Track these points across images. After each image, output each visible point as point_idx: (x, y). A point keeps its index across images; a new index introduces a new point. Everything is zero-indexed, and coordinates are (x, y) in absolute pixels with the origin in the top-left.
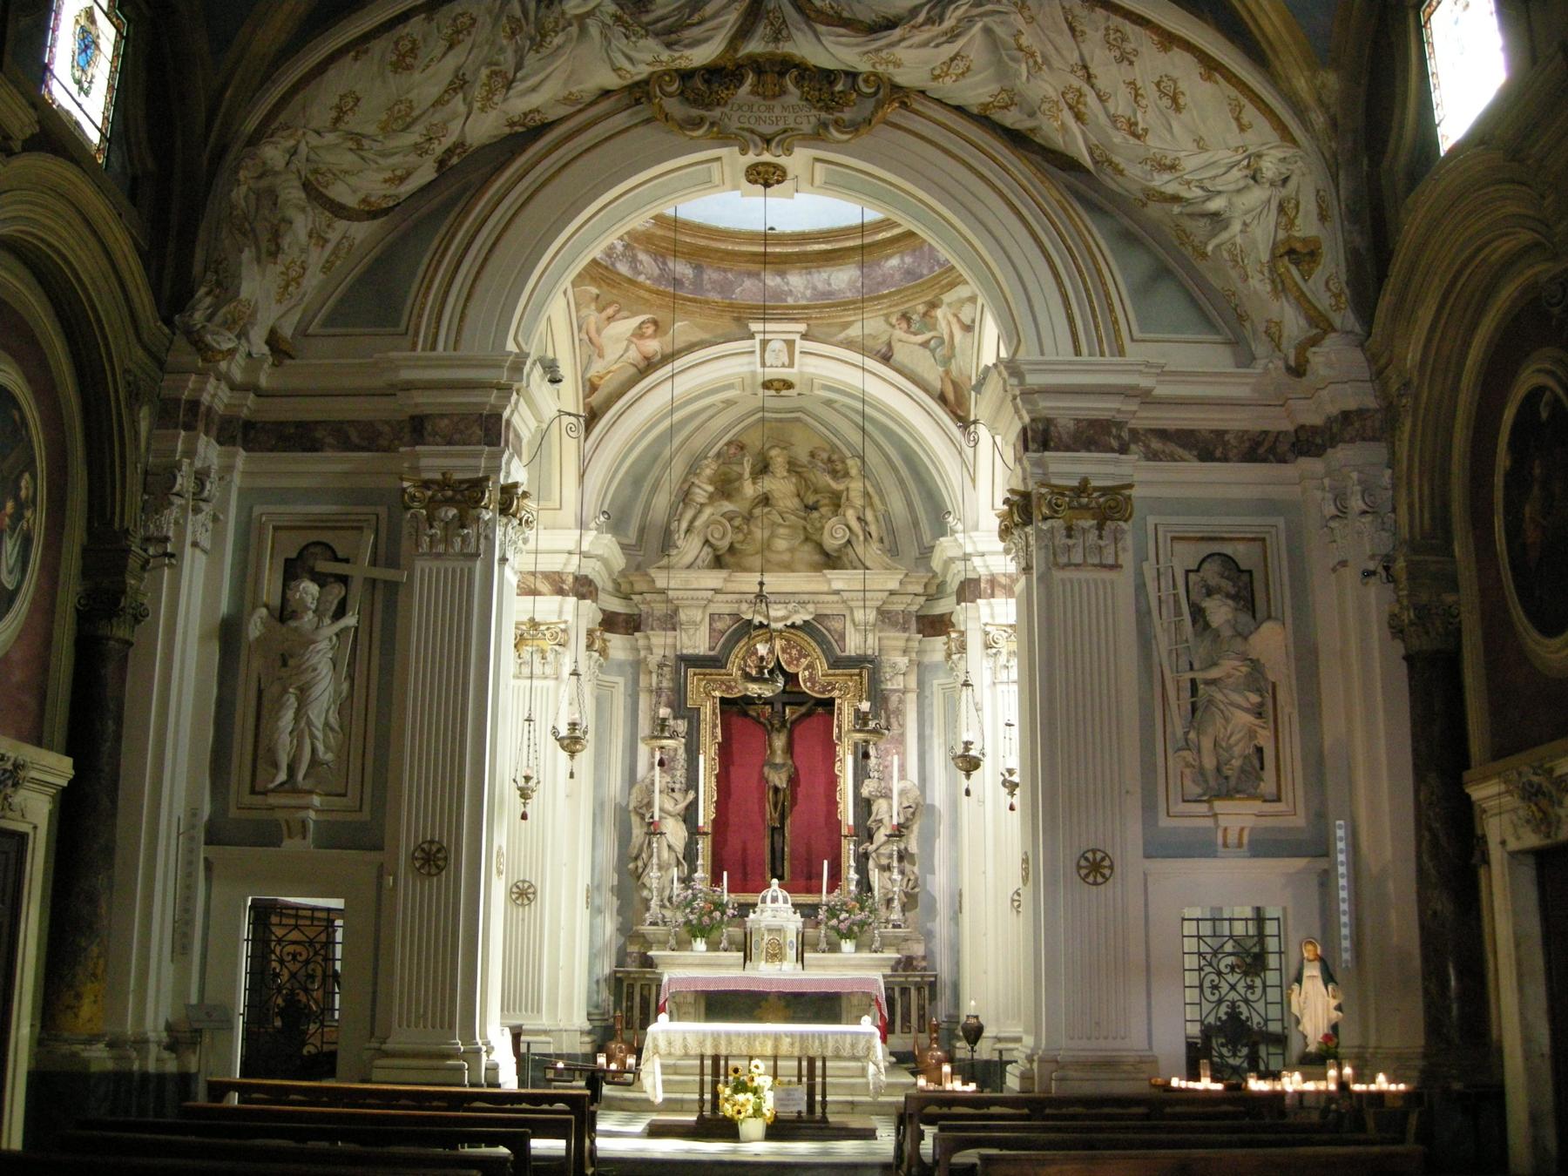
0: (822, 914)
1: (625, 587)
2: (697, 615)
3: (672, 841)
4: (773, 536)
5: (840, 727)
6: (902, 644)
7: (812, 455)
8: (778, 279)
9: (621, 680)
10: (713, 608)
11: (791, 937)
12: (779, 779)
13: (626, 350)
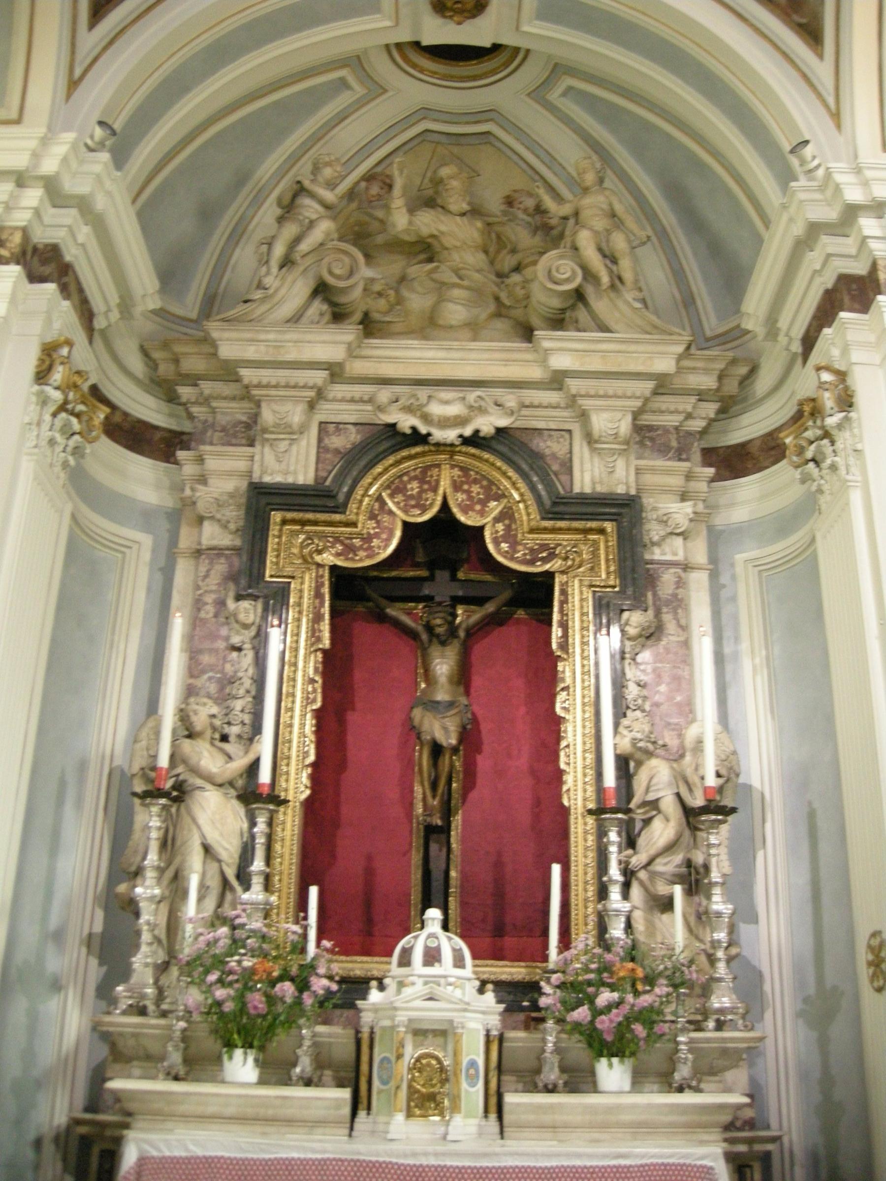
0: (549, 998)
1: (165, 369)
2: (296, 414)
3: (213, 837)
4: (441, 300)
5: (564, 625)
6: (676, 481)
7: (509, 202)
9: (146, 540)
10: (327, 412)
11: (473, 1051)
12: (443, 730)
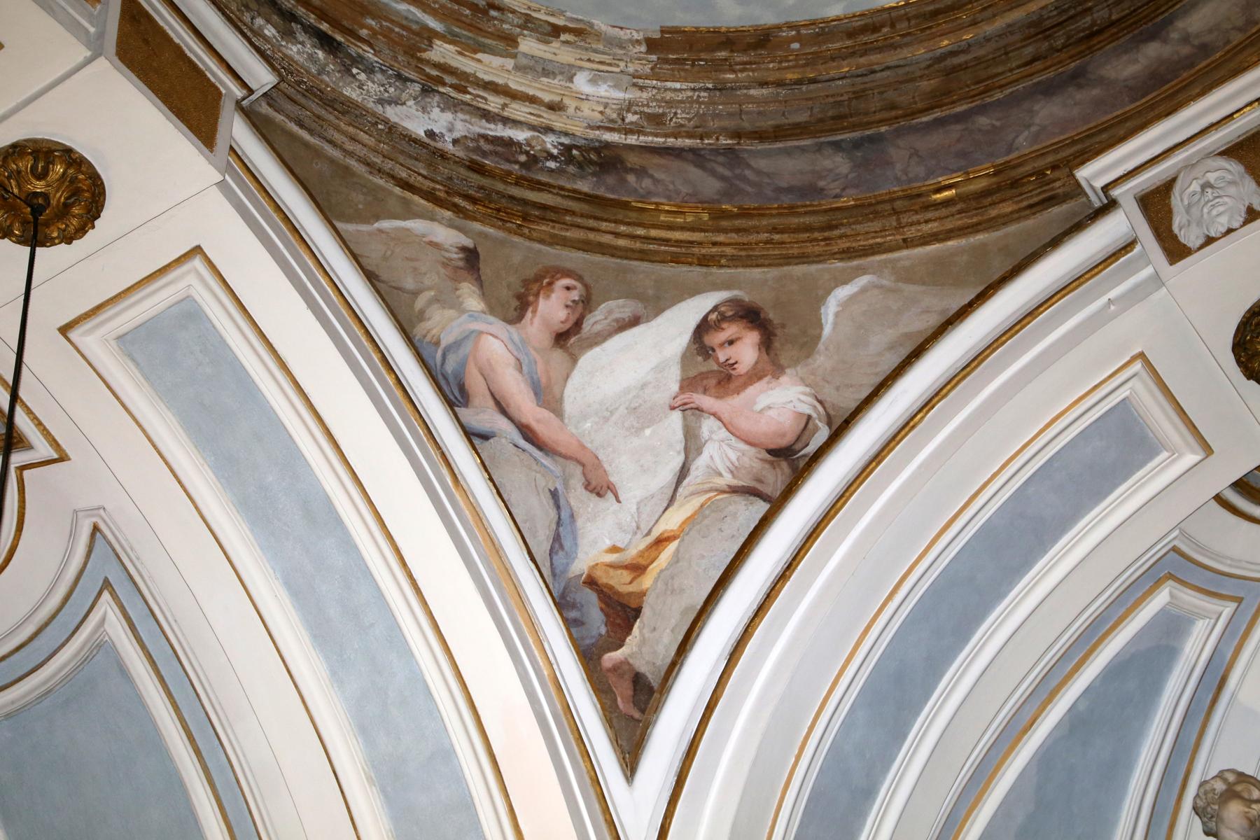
8: (1152, 51)
13: (692, 445)
